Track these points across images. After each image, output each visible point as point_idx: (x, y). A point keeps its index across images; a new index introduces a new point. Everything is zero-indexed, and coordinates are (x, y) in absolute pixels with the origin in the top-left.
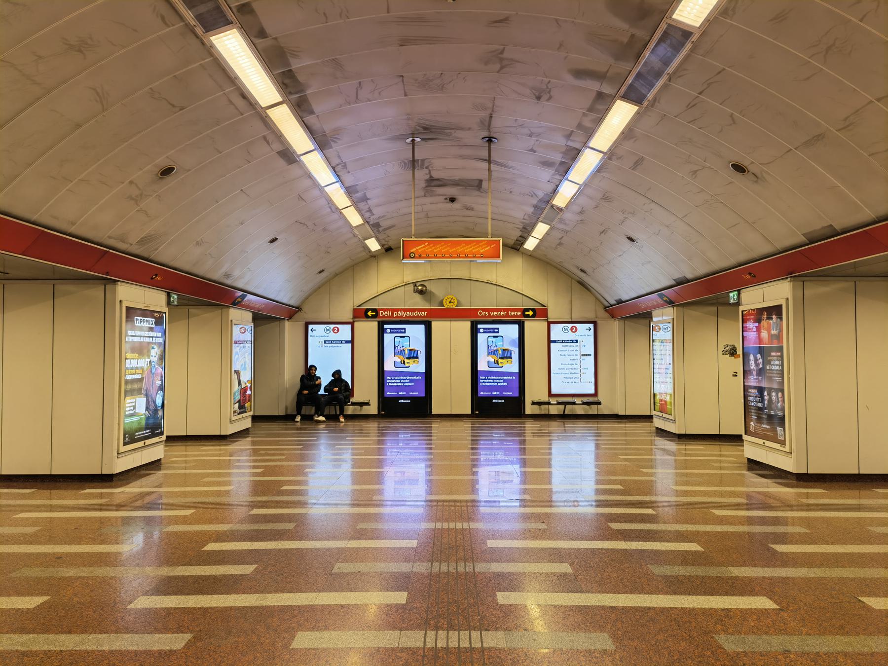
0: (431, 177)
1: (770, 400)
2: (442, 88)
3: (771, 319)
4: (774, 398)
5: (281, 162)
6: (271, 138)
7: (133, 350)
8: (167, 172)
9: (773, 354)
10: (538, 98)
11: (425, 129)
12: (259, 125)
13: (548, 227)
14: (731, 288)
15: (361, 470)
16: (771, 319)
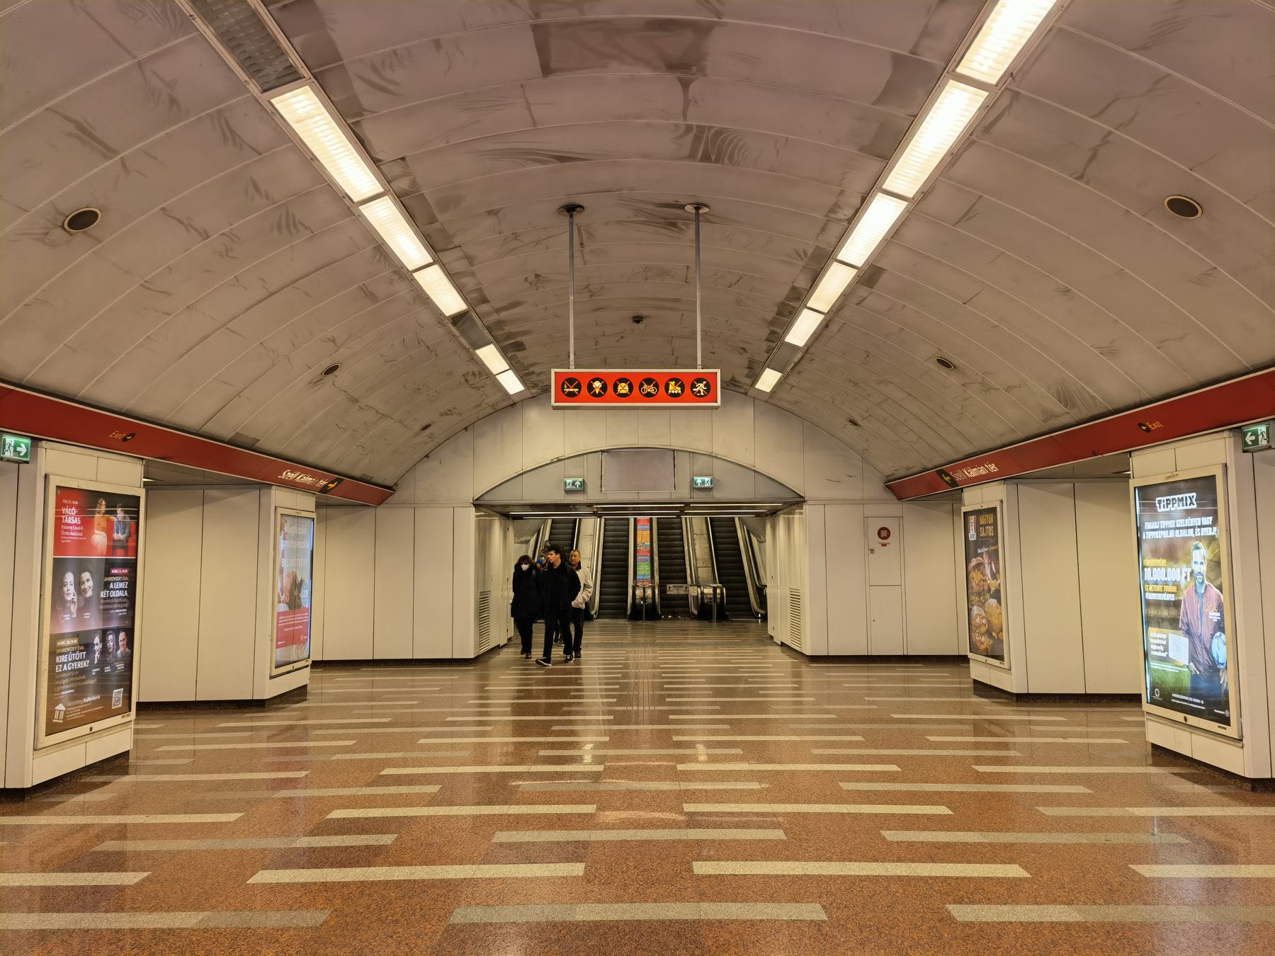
0: (685, 85)
1: (105, 650)
2: (646, 268)
3: (114, 513)
4: (111, 644)
5: (884, 280)
6: (854, 300)
7: (1156, 554)
8: (944, 363)
9: (115, 571)
10: (537, 276)
11: (674, 225)
12: (846, 313)
13: (478, 352)
14: (19, 427)
15: (763, 716)
16: (114, 513)
